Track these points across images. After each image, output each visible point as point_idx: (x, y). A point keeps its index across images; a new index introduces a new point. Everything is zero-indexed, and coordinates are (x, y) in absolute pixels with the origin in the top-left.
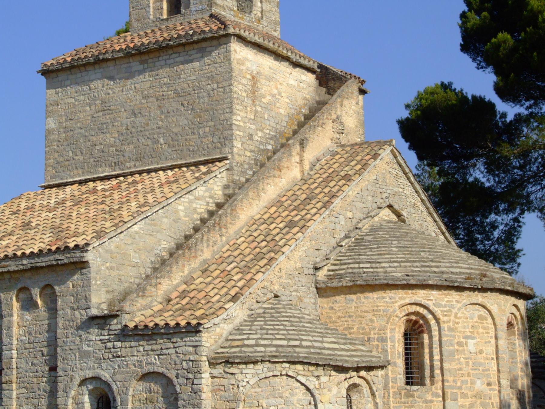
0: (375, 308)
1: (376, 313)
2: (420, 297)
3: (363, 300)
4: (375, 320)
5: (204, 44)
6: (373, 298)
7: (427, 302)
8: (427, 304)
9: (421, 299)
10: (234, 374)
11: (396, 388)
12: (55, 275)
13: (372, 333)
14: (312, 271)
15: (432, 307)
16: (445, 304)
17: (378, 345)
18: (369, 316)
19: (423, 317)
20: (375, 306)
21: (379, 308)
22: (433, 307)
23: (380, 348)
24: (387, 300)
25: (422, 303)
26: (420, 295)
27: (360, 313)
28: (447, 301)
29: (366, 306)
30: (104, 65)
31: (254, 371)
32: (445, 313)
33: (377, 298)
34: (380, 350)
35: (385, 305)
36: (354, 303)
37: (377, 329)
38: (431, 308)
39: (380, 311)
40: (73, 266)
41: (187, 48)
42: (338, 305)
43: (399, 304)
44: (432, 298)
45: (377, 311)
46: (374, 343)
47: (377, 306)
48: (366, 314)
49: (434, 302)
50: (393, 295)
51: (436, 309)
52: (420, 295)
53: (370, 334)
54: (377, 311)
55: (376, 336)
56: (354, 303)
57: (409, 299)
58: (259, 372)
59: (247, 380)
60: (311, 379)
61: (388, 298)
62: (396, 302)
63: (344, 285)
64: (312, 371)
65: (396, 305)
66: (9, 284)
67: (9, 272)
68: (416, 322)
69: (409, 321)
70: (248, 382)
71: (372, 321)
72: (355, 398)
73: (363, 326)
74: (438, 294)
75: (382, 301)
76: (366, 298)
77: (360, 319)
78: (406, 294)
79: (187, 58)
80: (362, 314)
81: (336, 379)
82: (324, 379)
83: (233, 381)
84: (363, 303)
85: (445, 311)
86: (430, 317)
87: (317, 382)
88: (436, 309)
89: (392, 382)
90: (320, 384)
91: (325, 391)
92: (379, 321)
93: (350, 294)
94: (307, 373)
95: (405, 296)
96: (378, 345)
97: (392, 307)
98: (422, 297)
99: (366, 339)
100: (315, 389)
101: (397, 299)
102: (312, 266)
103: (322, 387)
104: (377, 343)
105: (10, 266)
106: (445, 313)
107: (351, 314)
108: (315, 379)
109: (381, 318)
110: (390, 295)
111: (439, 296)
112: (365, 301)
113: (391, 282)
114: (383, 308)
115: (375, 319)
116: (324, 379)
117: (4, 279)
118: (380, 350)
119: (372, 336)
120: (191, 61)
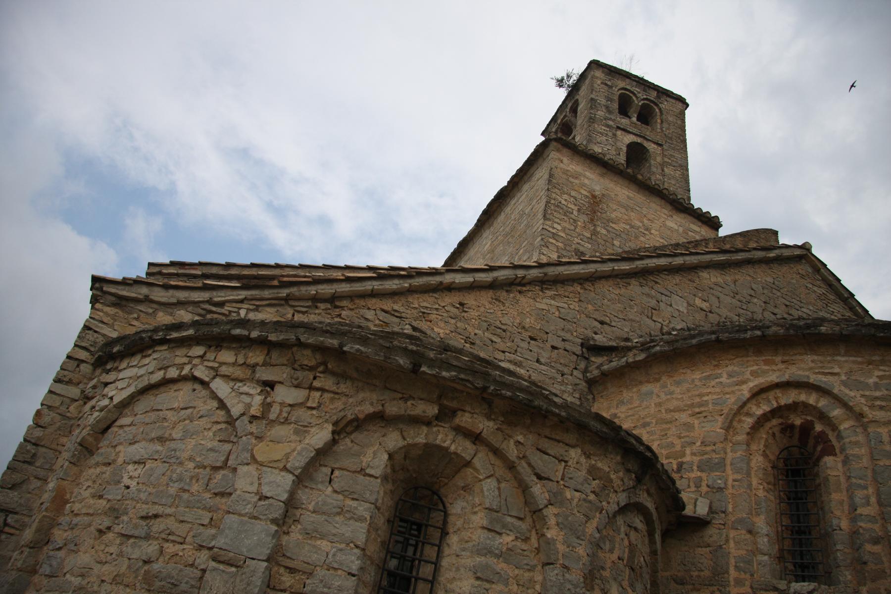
0: (697, 400)
1: (697, 410)
2: (804, 370)
3: (673, 388)
4: (696, 426)
6: (693, 380)
7: (824, 378)
8: (825, 382)
9: (807, 373)
11: (748, 583)
13: (688, 451)
14: (578, 350)
15: (838, 389)
16: (876, 384)
17: (700, 479)
18: (684, 417)
19: (822, 416)
20: (696, 396)
21: (706, 398)
22: (843, 388)
23: (704, 484)
24: (724, 379)
25: (811, 381)
26: (802, 366)
27: (664, 415)
28: (880, 378)
29: (677, 399)
32: (878, 403)
33: (700, 380)
34: (704, 489)
35: (718, 390)
36: (654, 397)
37: (698, 444)
38: (835, 391)
39: (708, 404)
42: (623, 408)
43: (751, 384)
44: (836, 370)
45: (700, 405)
46: (692, 475)
47: (700, 395)
48: (676, 415)
49: (843, 378)
50: (736, 368)
51: (852, 394)
52: (805, 366)
53: (684, 455)
54: (700, 405)
55: (696, 459)
56: (654, 397)
57: (778, 374)
60: (245, 389)
61: (725, 375)
62: (744, 382)
63: (631, 360)
64: (254, 367)
65: (745, 391)
68: (806, 429)
69: (787, 429)
71: (689, 427)
72: (459, 511)
73: (670, 440)
74: (854, 362)
75: (713, 383)
76: (678, 383)
77: (665, 426)
78: (766, 362)
80: (669, 416)
81: (339, 404)
82: (285, 394)
84: (672, 393)
85: (877, 398)
86: (836, 412)
87: (258, 399)
88: (852, 394)
89: (737, 567)
90: (266, 406)
91: (280, 431)
92: (703, 424)
93: (648, 382)
94: (238, 372)
95: (767, 368)
96: (700, 479)
97: (733, 392)
98: (811, 369)
99: (675, 467)
100: (246, 419)
101: (748, 375)
102: (580, 341)
103: (272, 416)
104: (699, 474)
106: (878, 403)
107: (648, 420)
108: (255, 390)
109: (710, 418)
110: (730, 368)
111: (855, 366)
112: (678, 390)
113: (724, 336)
114: (715, 397)
115: (696, 422)
116: (285, 394)
118: (704, 489)
119: (687, 458)
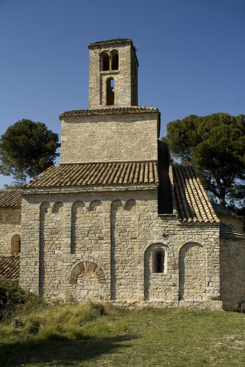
5: (144, 115)
10: (228, 245)
12: (136, 195)
30: (93, 117)
31: (234, 244)
40: (148, 191)
41: (136, 115)
58: (236, 245)
59: (232, 248)
66: (108, 197)
67: (111, 191)
70: (232, 249)
79: (135, 119)
83: (227, 248)
105: (112, 189)
117: (105, 195)
120: (138, 121)
